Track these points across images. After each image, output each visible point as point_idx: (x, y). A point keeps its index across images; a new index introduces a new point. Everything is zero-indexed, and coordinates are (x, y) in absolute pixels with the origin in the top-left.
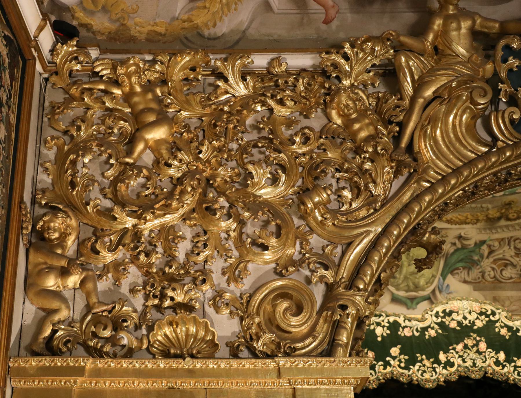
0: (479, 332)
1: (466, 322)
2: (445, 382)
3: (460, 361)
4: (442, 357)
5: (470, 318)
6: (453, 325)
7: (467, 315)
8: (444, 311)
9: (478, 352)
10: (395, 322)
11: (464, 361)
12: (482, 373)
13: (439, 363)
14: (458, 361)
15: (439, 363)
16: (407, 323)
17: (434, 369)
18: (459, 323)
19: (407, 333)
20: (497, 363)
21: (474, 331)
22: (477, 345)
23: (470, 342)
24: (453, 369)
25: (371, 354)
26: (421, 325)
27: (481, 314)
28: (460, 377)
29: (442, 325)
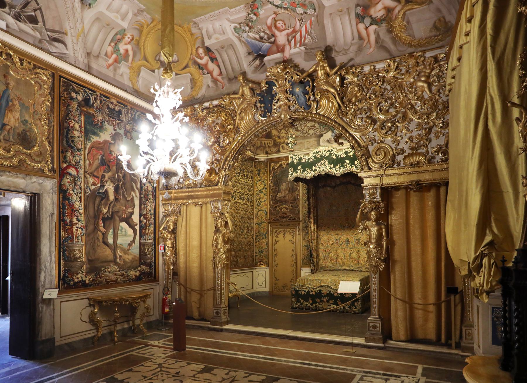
0: (327, 158)
1: (323, 155)
2: (313, 176)
3: (319, 169)
4: (314, 168)
5: (324, 153)
6: (319, 156)
7: (324, 152)
8: (316, 152)
9: (325, 165)
10: (301, 157)
11: (320, 169)
12: (325, 173)
13: (312, 170)
14: (318, 169)
15: (312, 170)
16: (304, 157)
17: (311, 172)
18: (321, 156)
19: (304, 161)
20: (331, 168)
21: (325, 158)
22: (325, 163)
23: (323, 162)
24: (316, 172)
25: (292, 169)
26: (309, 157)
27: (328, 151)
28: (318, 174)
29: (315, 157)
